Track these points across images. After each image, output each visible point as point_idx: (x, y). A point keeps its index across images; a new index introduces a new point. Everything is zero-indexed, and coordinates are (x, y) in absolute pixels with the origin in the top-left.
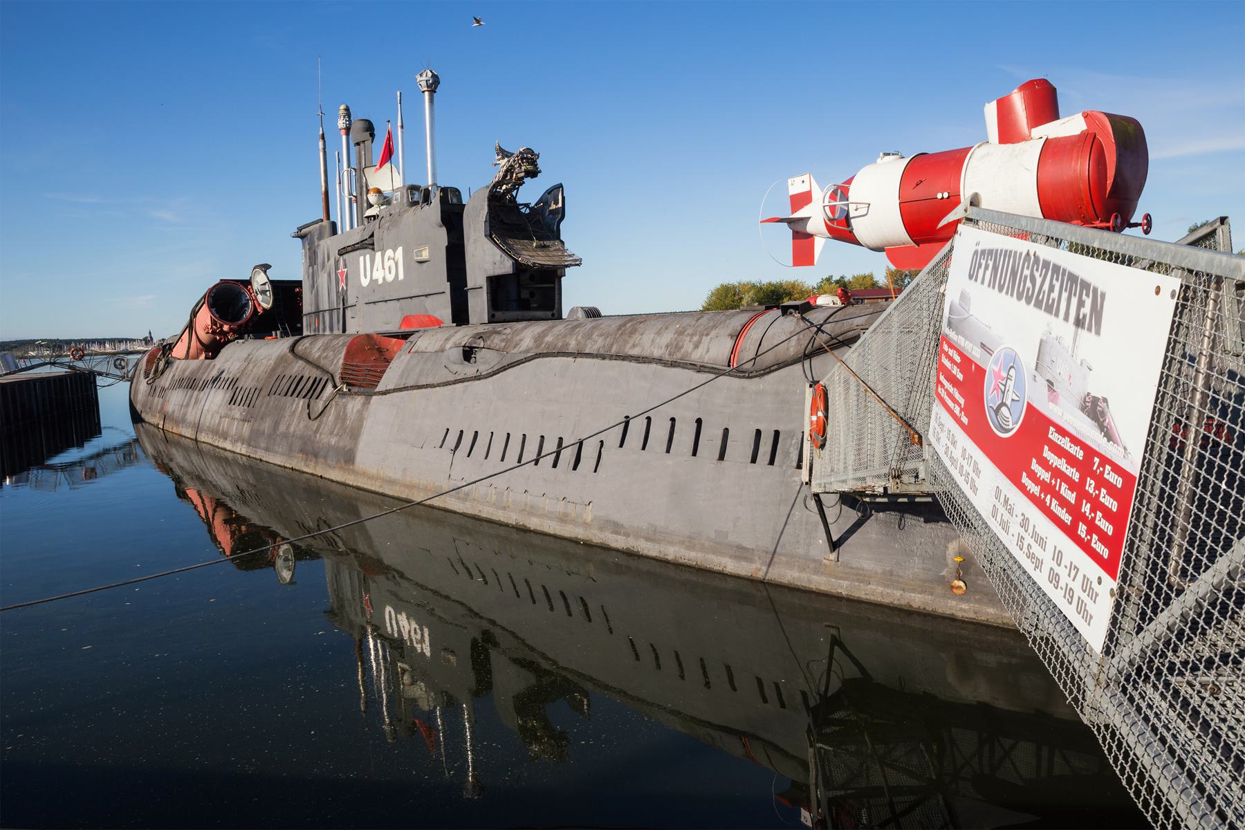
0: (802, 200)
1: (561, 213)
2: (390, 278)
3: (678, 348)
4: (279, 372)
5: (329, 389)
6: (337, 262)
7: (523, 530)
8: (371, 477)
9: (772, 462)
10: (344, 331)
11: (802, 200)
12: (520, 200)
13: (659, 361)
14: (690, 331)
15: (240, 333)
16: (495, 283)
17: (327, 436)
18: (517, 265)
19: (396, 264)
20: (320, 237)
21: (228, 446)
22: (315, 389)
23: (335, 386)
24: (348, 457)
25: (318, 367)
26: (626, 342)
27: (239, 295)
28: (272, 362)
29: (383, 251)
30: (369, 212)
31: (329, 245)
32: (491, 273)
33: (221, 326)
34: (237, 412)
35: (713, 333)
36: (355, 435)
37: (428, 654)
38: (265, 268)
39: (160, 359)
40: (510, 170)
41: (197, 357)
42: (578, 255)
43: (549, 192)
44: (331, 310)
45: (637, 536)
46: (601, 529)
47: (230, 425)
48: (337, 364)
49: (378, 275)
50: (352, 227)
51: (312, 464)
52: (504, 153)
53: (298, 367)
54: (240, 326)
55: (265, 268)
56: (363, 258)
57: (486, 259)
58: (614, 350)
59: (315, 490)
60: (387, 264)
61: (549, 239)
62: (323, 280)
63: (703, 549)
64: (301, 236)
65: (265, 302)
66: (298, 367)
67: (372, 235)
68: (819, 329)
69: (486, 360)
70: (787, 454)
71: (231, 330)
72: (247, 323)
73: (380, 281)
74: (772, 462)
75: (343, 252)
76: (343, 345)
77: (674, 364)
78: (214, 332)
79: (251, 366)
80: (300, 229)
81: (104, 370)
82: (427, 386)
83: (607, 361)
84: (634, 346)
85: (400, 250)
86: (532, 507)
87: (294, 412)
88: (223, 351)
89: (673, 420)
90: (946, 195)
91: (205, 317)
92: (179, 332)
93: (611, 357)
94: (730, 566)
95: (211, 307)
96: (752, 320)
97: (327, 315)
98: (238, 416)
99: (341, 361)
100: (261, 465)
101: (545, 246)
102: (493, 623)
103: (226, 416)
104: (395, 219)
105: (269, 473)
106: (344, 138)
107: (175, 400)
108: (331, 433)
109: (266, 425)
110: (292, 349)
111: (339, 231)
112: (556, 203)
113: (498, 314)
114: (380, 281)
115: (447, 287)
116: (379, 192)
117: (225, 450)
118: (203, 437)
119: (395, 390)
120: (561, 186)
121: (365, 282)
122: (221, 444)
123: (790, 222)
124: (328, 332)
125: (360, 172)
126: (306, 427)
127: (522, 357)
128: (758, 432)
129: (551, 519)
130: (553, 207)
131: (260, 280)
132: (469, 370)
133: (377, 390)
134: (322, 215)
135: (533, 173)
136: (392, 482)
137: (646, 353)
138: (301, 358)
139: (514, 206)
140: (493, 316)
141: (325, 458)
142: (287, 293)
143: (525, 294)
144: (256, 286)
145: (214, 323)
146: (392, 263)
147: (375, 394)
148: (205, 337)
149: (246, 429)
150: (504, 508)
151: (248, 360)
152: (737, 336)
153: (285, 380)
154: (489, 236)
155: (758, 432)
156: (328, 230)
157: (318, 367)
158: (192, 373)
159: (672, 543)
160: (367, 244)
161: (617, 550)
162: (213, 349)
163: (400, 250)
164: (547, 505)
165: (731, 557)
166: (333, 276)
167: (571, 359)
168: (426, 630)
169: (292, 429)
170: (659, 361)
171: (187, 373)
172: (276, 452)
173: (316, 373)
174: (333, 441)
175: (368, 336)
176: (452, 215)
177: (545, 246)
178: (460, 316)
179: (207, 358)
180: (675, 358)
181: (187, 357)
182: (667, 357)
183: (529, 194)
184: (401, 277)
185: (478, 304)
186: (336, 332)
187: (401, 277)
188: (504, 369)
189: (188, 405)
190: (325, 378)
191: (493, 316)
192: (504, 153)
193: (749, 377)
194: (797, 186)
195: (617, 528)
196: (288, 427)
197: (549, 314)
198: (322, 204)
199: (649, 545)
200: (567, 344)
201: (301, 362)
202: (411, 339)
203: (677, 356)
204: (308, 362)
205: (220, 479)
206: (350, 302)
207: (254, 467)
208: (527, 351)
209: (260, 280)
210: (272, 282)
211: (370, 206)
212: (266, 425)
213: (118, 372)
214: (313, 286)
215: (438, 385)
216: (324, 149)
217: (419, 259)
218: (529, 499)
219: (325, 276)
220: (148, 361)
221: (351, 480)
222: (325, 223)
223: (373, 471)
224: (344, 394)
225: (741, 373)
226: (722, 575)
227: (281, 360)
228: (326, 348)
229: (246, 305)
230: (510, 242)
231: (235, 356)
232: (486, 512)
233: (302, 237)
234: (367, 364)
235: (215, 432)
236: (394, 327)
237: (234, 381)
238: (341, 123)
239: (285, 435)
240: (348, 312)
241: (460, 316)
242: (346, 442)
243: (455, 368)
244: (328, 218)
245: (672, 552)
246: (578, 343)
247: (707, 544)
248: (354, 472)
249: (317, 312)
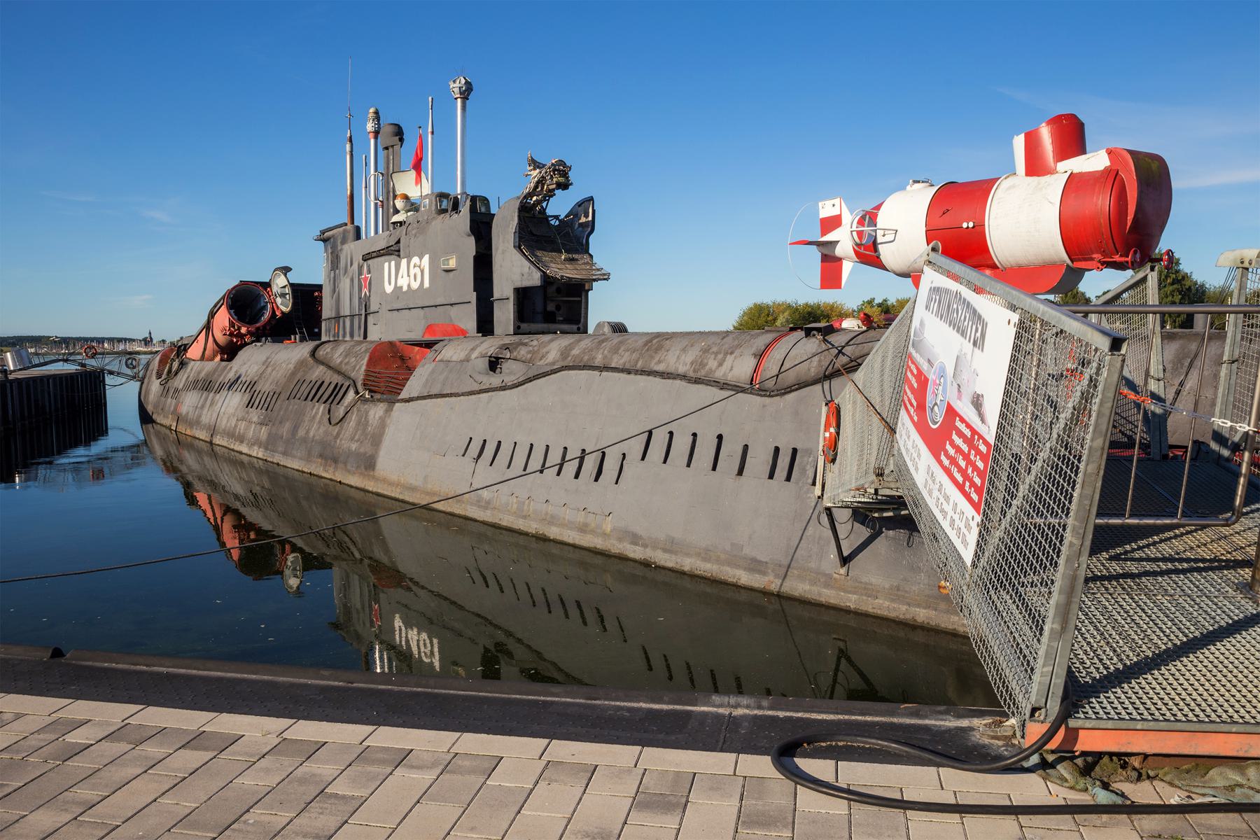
0: (832, 223)
1: (591, 226)
2: (415, 285)
3: (703, 365)
5: (351, 395)
6: (360, 268)
7: (543, 539)
8: (391, 484)
9: (788, 479)
10: (365, 337)
11: (832, 223)
12: (549, 212)
13: (683, 377)
14: (715, 349)
15: (258, 336)
16: (522, 295)
17: (348, 439)
18: (545, 277)
20: (344, 242)
21: (244, 449)
22: (336, 394)
23: (357, 392)
24: (369, 464)
25: (339, 373)
26: (652, 357)
27: (258, 297)
28: (291, 366)
29: (409, 258)
30: (396, 218)
31: (352, 250)
32: (519, 285)
33: (239, 328)
34: (255, 415)
35: (737, 353)
36: (377, 440)
37: (437, 664)
38: (286, 270)
39: (173, 360)
40: (541, 182)
41: (212, 359)
42: (607, 269)
43: (579, 204)
44: (352, 316)
45: (655, 548)
46: (620, 540)
47: (247, 428)
48: (359, 369)
49: (403, 282)
50: (376, 232)
51: (331, 469)
52: (535, 164)
53: (318, 372)
54: (258, 329)
55: (286, 270)
56: (388, 265)
57: (514, 269)
58: (639, 365)
59: (333, 496)
61: (577, 252)
62: (345, 284)
63: (718, 561)
64: (324, 238)
65: (284, 305)
66: (318, 372)
67: (398, 242)
68: (840, 352)
69: (512, 372)
70: (804, 471)
71: (249, 332)
72: (264, 326)
73: (405, 289)
74: (788, 479)
75: (367, 257)
76: (366, 351)
77: (697, 381)
78: (231, 334)
79: (270, 369)
80: (323, 232)
81: (115, 369)
82: (451, 395)
83: (632, 376)
84: (659, 362)
86: (552, 516)
87: (314, 417)
88: (241, 353)
89: (695, 435)
90: (971, 225)
91: (223, 318)
92: (195, 333)
93: (637, 372)
94: (744, 578)
95: (230, 308)
96: (776, 340)
97: (348, 321)
98: (255, 419)
99: (364, 368)
100: (278, 469)
101: (573, 260)
102: (509, 634)
103: (242, 420)
104: (422, 226)
105: (287, 478)
106: (372, 141)
107: (189, 402)
108: (352, 439)
109: (285, 429)
110: (313, 353)
111: (363, 236)
112: (587, 216)
113: (524, 326)
114: (405, 289)
116: (406, 197)
117: (241, 453)
118: (218, 440)
119: (418, 398)
120: (591, 199)
121: (389, 289)
122: (237, 447)
123: (818, 244)
124: (348, 338)
125: (387, 177)
126: (326, 432)
127: (548, 369)
128: (777, 450)
129: (571, 529)
130: (583, 220)
131: (280, 282)
132: (495, 380)
134: (346, 219)
135: (564, 186)
136: (413, 489)
137: (671, 369)
138: (323, 363)
139: (543, 218)
140: (519, 327)
141: (345, 463)
142: (307, 296)
143: (551, 307)
144: (275, 289)
145: (232, 324)
146: (417, 270)
147: (399, 401)
148: (221, 339)
149: (264, 433)
150: (525, 517)
151: (266, 363)
152: (760, 356)
153: (305, 385)
154: (518, 247)
155: (777, 450)
156: (351, 235)
158: (208, 375)
159: (688, 555)
160: (393, 251)
161: (634, 561)
162: (229, 351)
163: (426, 258)
164: (568, 515)
165: (745, 569)
167: (597, 373)
168: (435, 641)
169: (311, 434)
170: (683, 377)
171: (202, 375)
172: (294, 457)
173: (337, 379)
174: (354, 446)
175: (391, 344)
176: (481, 226)
177: (573, 260)
178: (485, 326)
179: (222, 360)
180: (699, 375)
181: (202, 358)
182: (691, 374)
183: (559, 206)
184: (427, 284)
185: (504, 315)
186: (356, 338)
187: (427, 284)
188: (530, 380)
189: (203, 406)
190: (347, 384)
191: (519, 327)
192: (535, 164)
193: (770, 396)
194: (827, 209)
195: (635, 539)
196: (308, 432)
197: (575, 327)
198: (347, 208)
199: (667, 556)
200: (594, 358)
201: (321, 367)
202: (436, 347)
203: (701, 374)
204: (329, 367)
205: (234, 483)
206: (373, 308)
207: (271, 472)
208: (553, 363)
209: (280, 282)
210: (292, 285)
211: (397, 211)
212: (285, 429)
213: (129, 372)
214: (334, 291)
215: (463, 394)
217: (446, 267)
218: (550, 509)
219: (348, 281)
220: (161, 361)
221: (370, 486)
222: (349, 227)
223: (394, 478)
224: (366, 400)
225: (763, 392)
226: (737, 587)
227: (301, 364)
228: (347, 354)
229: (264, 308)
230: (539, 253)
231: (252, 360)
232: (507, 520)
233: (325, 241)
234: (390, 371)
235: (231, 435)
236: (417, 335)
237: (252, 384)
238: (370, 126)
239: (304, 440)
240: (370, 318)
241: (485, 326)
242: (366, 448)
243: (480, 378)
244: (352, 222)
245: (688, 563)
246: (605, 358)
247: (723, 556)
248: (376, 479)
249: (338, 318)
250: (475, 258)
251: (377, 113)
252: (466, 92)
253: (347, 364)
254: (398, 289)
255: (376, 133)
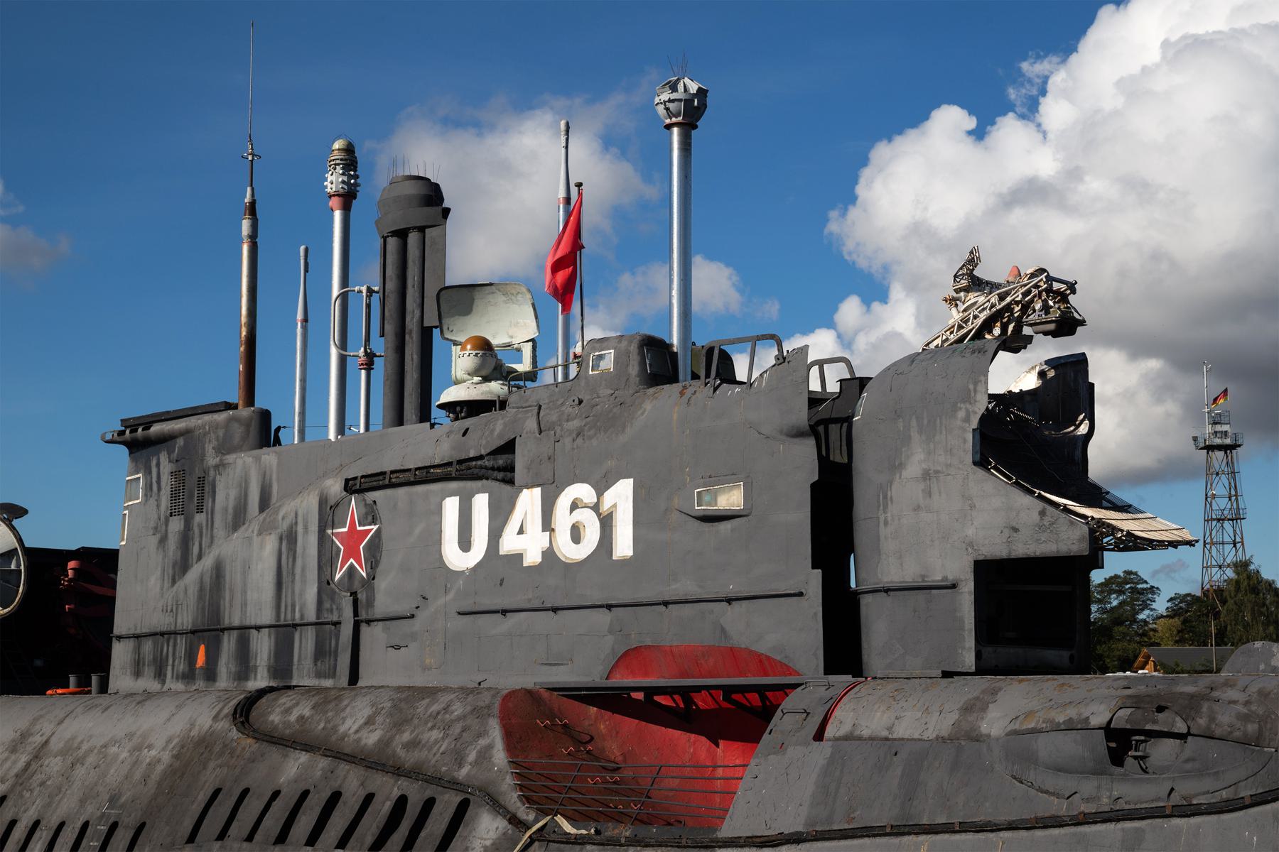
4: (211, 777)
6: (329, 513)
10: (354, 678)
19: (606, 522)
20: (225, 448)
23: (514, 821)
25: (398, 771)
32: (996, 548)
49: (526, 540)
50: (341, 429)
60: (563, 518)
64: (139, 439)
73: (533, 557)
76: (480, 713)
79: (54, 765)
80: (131, 424)
82: (965, 828)
85: (621, 495)
97: (263, 646)
99: (500, 756)
106: (338, 215)
111: (292, 437)
114: (533, 557)
115: (813, 581)
133: (725, 832)
157: (398, 771)
166: (309, 544)
175: (529, 692)
187: (624, 546)
190: (447, 803)
204: (338, 755)
206: (383, 603)
210: (31, 553)
216: (253, 237)
219: (270, 545)
227: (195, 751)
233: (135, 446)
236: (587, 669)
238: (334, 181)
244: (250, 398)
249: (209, 630)
250: (815, 487)
251: (349, 150)
252: (692, 114)
253: (413, 745)
254: (499, 565)
255: (348, 197)
